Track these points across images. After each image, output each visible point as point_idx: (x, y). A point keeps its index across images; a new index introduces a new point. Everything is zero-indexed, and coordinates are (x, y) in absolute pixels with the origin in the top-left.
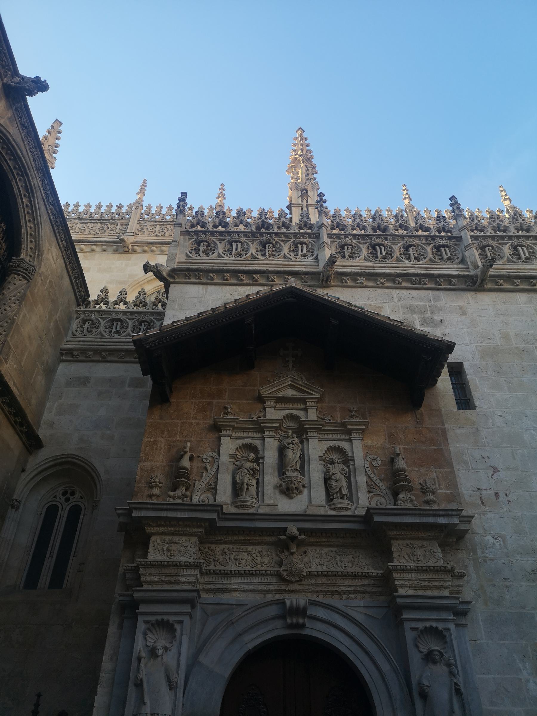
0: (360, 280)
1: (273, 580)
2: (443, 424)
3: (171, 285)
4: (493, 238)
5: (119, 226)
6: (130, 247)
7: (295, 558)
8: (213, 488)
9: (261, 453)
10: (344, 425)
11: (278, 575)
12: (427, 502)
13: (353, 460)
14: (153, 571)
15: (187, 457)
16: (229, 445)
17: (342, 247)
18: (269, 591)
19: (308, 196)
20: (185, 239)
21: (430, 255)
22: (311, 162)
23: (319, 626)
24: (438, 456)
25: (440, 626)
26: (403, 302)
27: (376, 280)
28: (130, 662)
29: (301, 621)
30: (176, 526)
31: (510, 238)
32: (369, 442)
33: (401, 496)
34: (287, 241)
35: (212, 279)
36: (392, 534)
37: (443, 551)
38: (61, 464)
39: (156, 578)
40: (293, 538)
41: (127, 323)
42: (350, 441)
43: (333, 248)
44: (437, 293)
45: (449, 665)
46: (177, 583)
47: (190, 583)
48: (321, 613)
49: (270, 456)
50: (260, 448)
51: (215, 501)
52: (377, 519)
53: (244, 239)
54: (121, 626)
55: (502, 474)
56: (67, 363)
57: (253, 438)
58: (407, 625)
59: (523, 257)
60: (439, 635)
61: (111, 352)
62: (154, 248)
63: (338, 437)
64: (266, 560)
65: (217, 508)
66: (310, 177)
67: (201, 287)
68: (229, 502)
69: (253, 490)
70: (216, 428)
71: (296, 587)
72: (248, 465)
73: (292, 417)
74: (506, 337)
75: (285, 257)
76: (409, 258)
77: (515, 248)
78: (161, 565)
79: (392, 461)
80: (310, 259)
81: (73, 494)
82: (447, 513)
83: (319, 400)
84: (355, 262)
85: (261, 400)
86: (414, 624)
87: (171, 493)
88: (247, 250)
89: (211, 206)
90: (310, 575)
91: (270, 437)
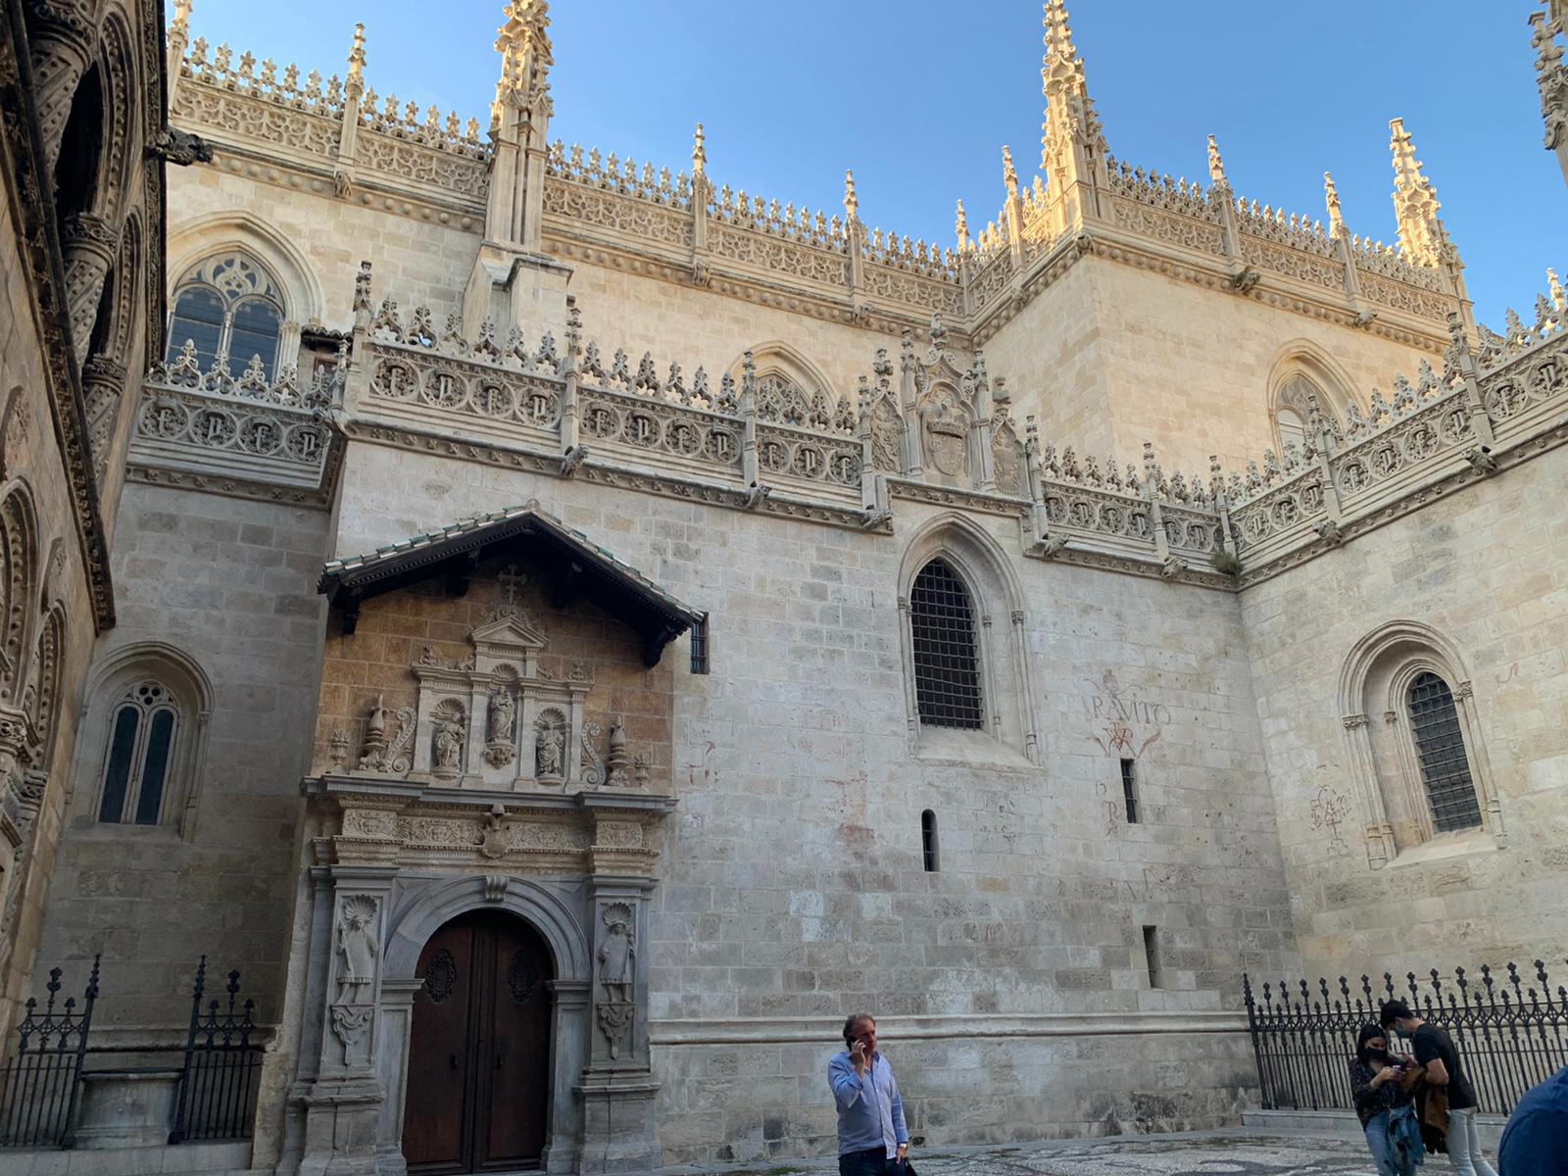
0: (612, 477)
1: (473, 856)
3: (350, 443)
4: (782, 432)
7: (498, 835)
8: (410, 753)
9: (467, 713)
10: (566, 685)
11: (480, 852)
12: (638, 779)
13: (571, 727)
14: (351, 848)
15: (380, 713)
17: (595, 412)
18: (468, 866)
19: (531, 129)
20: (368, 357)
21: (703, 446)
22: (544, 36)
23: (516, 900)
24: (658, 729)
25: (627, 902)
26: (658, 518)
27: (631, 481)
28: (329, 931)
29: (499, 896)
30: (374, 799)
31: (801, 436)
33: (615, 774)
34: (520, 387)
35: (411, 444)
36: (598, 816)
37: (644, 830)
38: (142, 654)
39: (354, 855)
40: (498, 816)
41: (232, 421)
42: (571, 703)
43: (583, 411)
44: (701, 507)
45: (629, 936)
46: (376, 859)
47: (390, 860)
48: (518, 889)
49: (478, 718)
50: (466, 706)
51: (412, 768)
52: (588, 803)
53: (457, 373)
54: (312, 896)
55: (718, 751)
56: (135, 486)
57: (458, 693)
58: (598, 901)
59: (808, 467)
60: (625, 910)
61: (213, 478)
63: (558, 698)
64: (466, 834)
65: (422, 786)
66: (539, 82)
67: (394, 451)
68: (428, 770)
69: (456, 757)
70: (414, 676)
72: (453, 727)
73: (506, 668)
74: (761, 583)
75: (514, 417)
76: (676, 445)
77: (803, 452)
79: (612, 731)
80: (549, 426)
81: (156, 692)
82: (656, 799)
83: (542, 650)
84: (609, 442)
85: (470, 642)
86: (604, 901)
87: (364, 760)
89: (335, 79)
91: (481, 693)
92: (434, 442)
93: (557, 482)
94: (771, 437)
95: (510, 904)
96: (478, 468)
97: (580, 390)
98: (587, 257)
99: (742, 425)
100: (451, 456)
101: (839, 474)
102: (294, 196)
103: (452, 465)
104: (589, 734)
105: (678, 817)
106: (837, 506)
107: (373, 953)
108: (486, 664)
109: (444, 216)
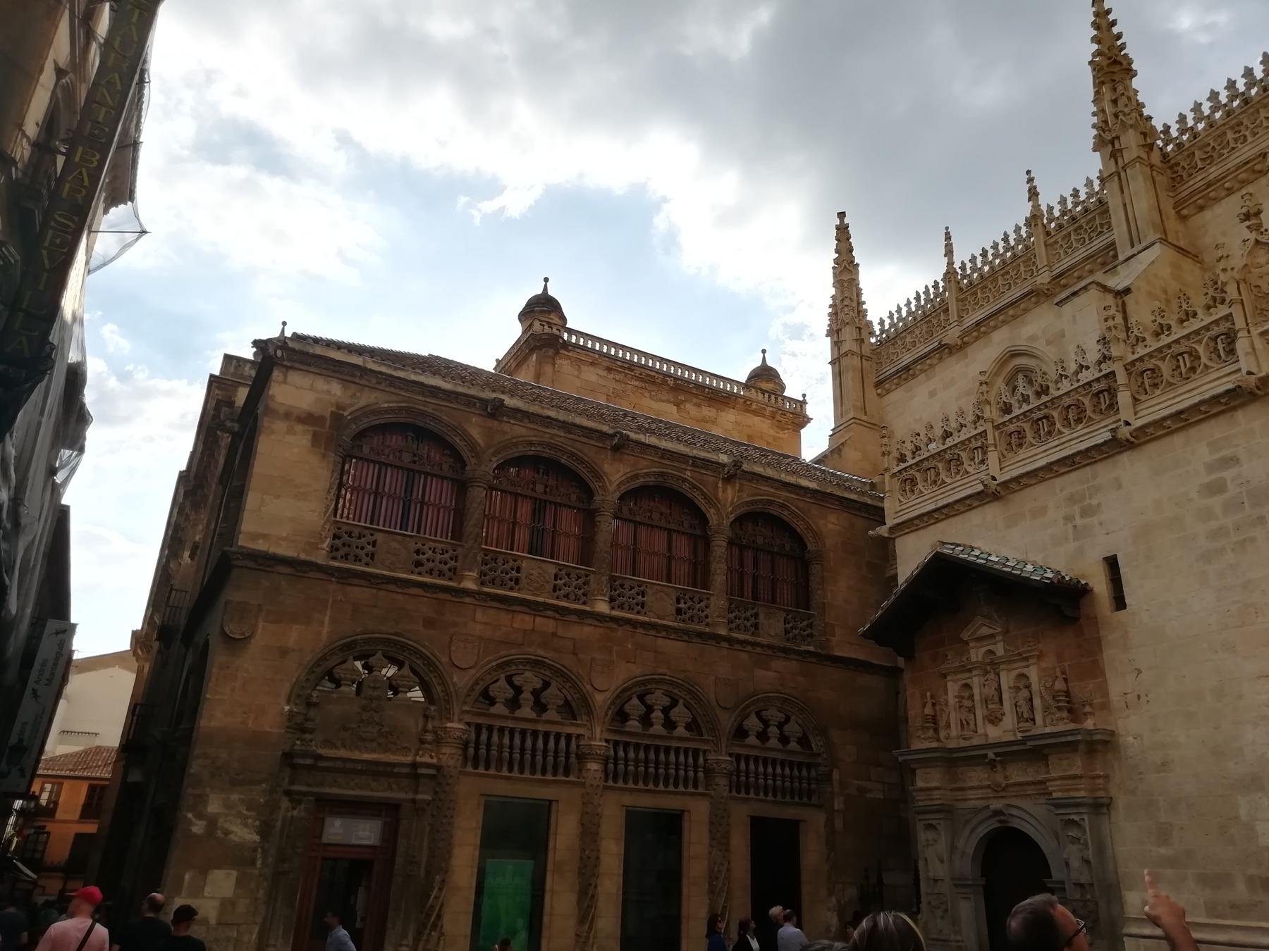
0: (1024, 481)
2: (1098, 632)
5: (942, 317)
6: (959, 342)
10: (1020, 654)
12: (1085, 714)
16: (953, 688)
25: (1076, 818)
31: (1169, 346)
32: (1044, 665)
36: (1046, 751)
48: (1014, 812)
52: (1030, 744)
53: (934, 463)
59: (1183, 370)
62: (983, 329)
66: (1121, 107)
69: (972, 723)
70: (945, 676)
71: (1004, 794)
73: (991, 652)
78: (922, 790)
84: (1023, 453)
88: (938, 474)
90: (1007, 786)
92: (925, 518)
93: (996, 504)
94: (1140, 366)
95: (1015, 823)
96: (952, 520)
97: (997, 427)
98: (1228, 189)
99: (1113, 373)
100: (938, 521)
101: (1219, 356)
102: (1029, 316)
103: (939, 525)
104: (1046, 688)
105: (1121, 740)
106: (1207, 396)
107: (942, 861)
108: (977, 654)
109: (1111, 253)
